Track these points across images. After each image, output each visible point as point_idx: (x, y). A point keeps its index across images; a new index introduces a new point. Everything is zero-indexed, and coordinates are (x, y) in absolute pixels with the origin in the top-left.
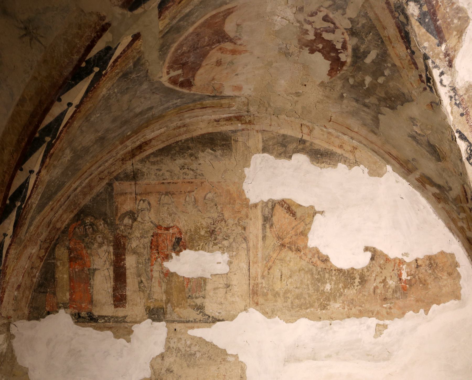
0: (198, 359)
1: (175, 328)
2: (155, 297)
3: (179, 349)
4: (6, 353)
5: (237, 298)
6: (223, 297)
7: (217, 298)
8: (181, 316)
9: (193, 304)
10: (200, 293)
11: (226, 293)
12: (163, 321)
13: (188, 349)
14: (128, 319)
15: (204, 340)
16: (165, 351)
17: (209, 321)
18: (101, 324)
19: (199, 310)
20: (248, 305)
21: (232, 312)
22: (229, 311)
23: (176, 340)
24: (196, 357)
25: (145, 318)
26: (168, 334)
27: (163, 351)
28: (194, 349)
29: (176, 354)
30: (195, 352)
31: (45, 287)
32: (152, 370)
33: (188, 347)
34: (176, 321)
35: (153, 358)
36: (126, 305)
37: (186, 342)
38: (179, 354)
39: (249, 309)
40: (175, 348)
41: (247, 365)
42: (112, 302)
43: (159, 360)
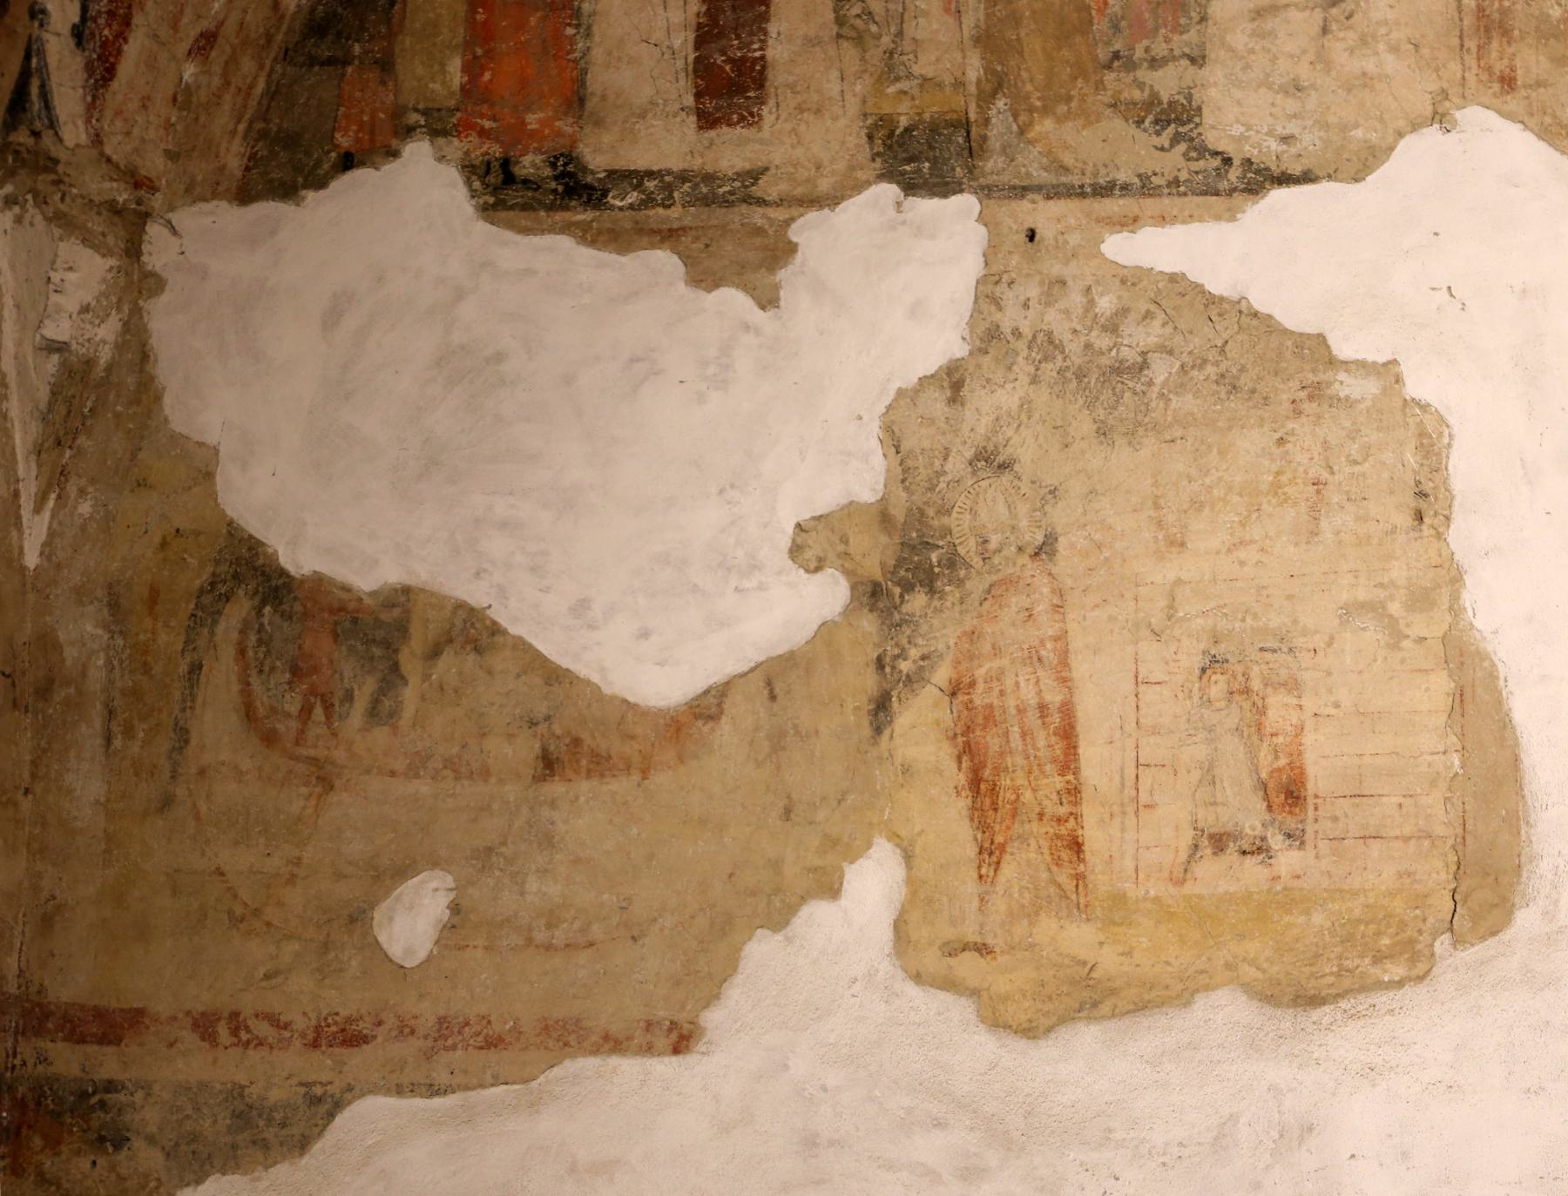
1: (1027, 226)
2: (924, 66)
3: (1051, 342)
4: (109, 369)
5: (1390, 59)
6: (1304, 52)
7: (1274, 59)
8: (1068, 160)
9: (1137, 95)
10: (1176, 38)
11: (1325, 30)
12: (961, 191)
13: (1102, 341)
14: (769, 188)
15: (1199, 288)
16: (971, 353)
17: (1223, 185)
18: (621, 214)
19: (1171, 130)
20: (1454, 91)
21: (1358, 133)
22: (1344, 128)
23: (1033, 291)
24: (1150, 383)
25: (861, 175)
26: (990, 255)
27: (960, 350)
28: (1139, 337)
29: (1032, 369)
30: (1144, 354)
31: (339, 34)
33: (1104, 328)
34: (1038, 188)
35: (900, 393)
36: (765, 110)
37: (1091, 303)
38: (1049, 370)
39: (1458, 115)
40: (1027, 331)
42: (690, 100)
43: (935, 402)
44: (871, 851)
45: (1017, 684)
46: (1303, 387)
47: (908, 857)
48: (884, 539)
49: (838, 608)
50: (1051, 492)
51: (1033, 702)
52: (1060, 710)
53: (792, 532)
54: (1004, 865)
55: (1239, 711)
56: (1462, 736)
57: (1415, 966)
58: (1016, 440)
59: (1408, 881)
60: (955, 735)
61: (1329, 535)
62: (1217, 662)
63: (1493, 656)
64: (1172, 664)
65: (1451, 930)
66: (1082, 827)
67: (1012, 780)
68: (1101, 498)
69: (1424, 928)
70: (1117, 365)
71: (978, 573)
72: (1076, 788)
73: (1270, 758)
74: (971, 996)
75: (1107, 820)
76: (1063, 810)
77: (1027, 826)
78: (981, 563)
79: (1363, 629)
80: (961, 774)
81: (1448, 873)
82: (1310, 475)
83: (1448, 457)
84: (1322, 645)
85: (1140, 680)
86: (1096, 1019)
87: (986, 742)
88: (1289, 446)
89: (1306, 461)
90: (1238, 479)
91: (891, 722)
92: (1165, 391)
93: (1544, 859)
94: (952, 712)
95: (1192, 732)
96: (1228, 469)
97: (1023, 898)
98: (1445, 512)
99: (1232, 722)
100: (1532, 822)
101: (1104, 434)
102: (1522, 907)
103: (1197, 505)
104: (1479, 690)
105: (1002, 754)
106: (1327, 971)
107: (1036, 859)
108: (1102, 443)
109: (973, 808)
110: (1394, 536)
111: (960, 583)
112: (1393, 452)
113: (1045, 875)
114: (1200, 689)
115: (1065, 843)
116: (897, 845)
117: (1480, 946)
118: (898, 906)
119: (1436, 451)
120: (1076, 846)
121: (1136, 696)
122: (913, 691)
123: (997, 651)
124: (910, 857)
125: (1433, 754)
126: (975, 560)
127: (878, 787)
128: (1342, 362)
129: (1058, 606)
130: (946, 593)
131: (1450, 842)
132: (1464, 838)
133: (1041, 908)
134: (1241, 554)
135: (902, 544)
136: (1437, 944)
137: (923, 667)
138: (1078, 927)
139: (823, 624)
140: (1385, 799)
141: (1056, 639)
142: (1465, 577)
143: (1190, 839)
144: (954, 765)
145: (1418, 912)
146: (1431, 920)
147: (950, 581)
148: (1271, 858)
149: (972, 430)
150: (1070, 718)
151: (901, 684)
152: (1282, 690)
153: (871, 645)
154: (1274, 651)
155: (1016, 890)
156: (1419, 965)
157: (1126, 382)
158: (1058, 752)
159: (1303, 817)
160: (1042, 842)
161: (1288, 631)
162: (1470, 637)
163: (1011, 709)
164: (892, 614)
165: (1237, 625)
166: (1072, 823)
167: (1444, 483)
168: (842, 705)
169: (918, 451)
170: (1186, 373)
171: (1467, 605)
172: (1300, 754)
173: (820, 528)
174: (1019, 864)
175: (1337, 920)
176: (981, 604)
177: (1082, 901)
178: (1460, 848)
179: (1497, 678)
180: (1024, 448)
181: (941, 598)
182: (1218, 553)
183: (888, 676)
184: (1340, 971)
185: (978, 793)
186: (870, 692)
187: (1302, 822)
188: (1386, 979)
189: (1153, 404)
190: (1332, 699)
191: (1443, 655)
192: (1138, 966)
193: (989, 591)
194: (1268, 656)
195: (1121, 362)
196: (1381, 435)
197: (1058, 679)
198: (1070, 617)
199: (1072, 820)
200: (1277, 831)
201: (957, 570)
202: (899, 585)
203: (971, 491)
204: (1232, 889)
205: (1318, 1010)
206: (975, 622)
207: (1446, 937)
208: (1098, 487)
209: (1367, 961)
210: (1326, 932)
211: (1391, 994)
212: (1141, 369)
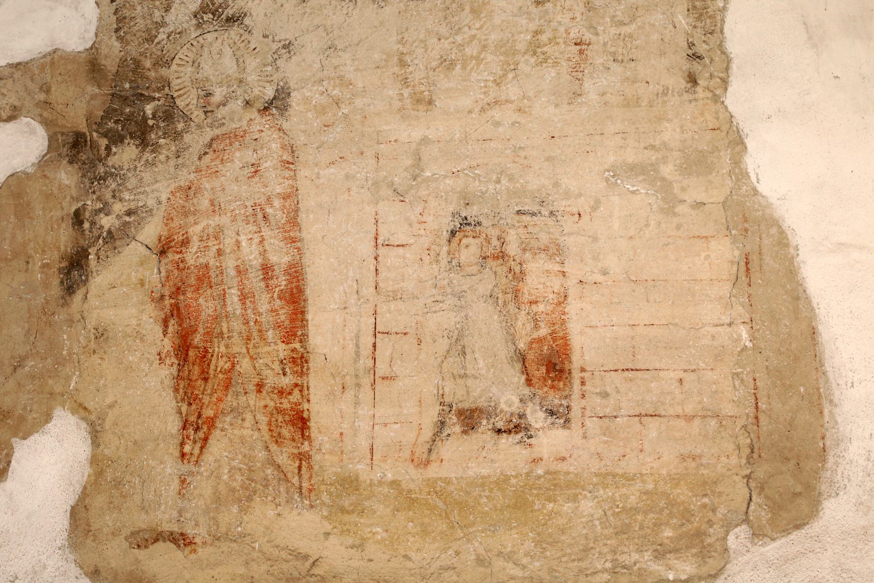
44: (49, 425)
45: (238, 243)
47: (95, 435)
50: (284, 47)
51: (257, 262)
55: (493, 276)
59: (693, 464)
60: (162, 297)
61: (593, 96)
66: (308, 401)
67: (227, 347)
68: (340, 53)
72: (302, 357)
73: (529, 326)
75: (338, 393)
76: (286, 381)
78: (203, 116)
79: (633, 192)
80: (166, 340)
81: (740, 457)
82: (572, 35)
85: (380, 241)
87: (199, 305)
89: (567, 21)
91: (86, 282)
95: (440, 298)
97: (235, 480)
98: (721, 75)
100: (836, 401)
102: (830, 496)
103: (447, 64)
104: (767, 259)
105: (216, 318)
106: (599, 567)
107: (252, 436)
109: (179, 377)
110: (665, 98)
111: (177, 136)
113: (261, 455)
114: (449, 253)
115: (287, 418)
117: (783, 540)
118: (79, 489)
119: (712, 13)
120: (301, 422)
121: (376, 258)
122: (115, 248)
123: (215, 207)
124: (97, 432)
125: (717, 326)
126: (196, 113)
127: (65, 353)
129: (288, 163)
130: (159, 146)
132: (756, 418)
133: (255, 492)
134: (496, 113)
136: (731, 538)
137: (129, 223)
138: (299, 514)
139: (12, 175)
140: (661, 373)
141: (286, 197)
142: (746, 141)
143: (436, 415)
144: (158, 329)
146: (722, 510)
147: (164, 134)
148: (530, 437)
151: (101, 241)
152: (543, 255)
153: (68, 198)
154: (533, 214)
155: (226, 471)
158: (283, 317)
159: (566, 393)
160: (258, 417)
163: (229, 270)
166: (296, 395)
168: (27, 262)
172: (563, 322)
173: (16, 76)
174: (231, 440)
176: (200, 158)
177: (305, 485)
181: (153, 151)
182: (470, 112)
183: (87, 232)
184: (615, 567)
185: (185, 360)
186: (63, 248)
187: (566, 397)
191: (724, 221)
192: (371, 560)
193: (210, 145)
194: (526, 219)
197: (286, 239)
198: (303, 172)
199: (296, 392)
200: (538, 408)
201: (173, 123)
202: (106, 136)
203: (195, 43)
204: (484, 472)
206: (192, 176)
207: (742, 531)
209: (647, 555)
210: (597, 523)
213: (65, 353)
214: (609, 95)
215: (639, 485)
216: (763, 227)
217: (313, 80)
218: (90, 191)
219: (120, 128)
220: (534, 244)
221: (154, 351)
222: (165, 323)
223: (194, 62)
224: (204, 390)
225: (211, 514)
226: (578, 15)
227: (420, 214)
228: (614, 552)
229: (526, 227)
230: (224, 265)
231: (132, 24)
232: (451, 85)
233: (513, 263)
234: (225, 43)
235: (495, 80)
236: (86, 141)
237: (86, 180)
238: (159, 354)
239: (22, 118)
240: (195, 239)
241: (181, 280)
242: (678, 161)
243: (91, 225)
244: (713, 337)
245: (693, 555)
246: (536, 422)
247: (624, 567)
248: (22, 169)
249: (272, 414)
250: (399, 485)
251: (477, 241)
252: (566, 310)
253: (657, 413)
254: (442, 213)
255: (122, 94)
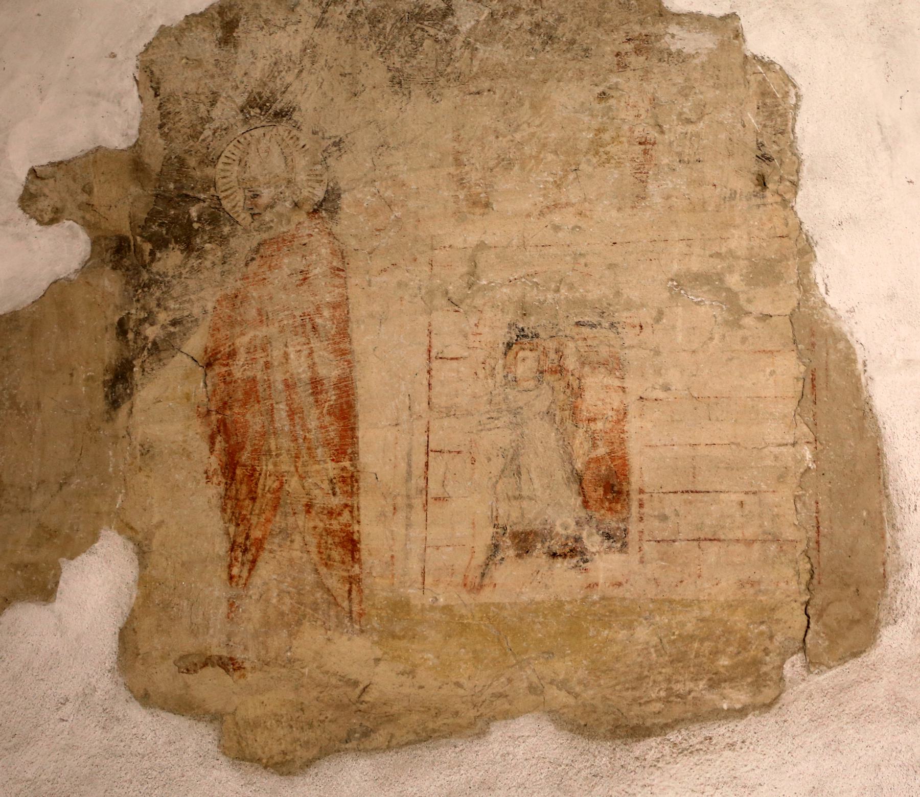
0: (467, 44)
24: (455, 31)
29: (318, 12)
32: (154, 103)
35: (163, 31)
41: (798, 80)
44: (96, 545)
45: (286, 356)
46: (629, 40)
47: (142, 553)
48: (135, 190)
49: (75, 265)
50: (335, 144)
51: (306, 376)
52: (336, 387)
53: (24, 179)
54: (260, 564)
55: (550, 392)
56: (814, 426)
57: (760, 692)
58: (296, 86)
59: (752, 591)
60: (209, 412)
61: (657, 200)
62: (526, 336)
63: (849, 337)
64: (471, 337)
65: (803, 649)
66: (359, 522)
67: (275, 465)
68: (393, 152)
69: (771, 647)
70: (417, 10)
71: (245, 230)
72: (352, 476)
73: (587, 446)
74: (211, 721)
75: (390, 514)
76: (336, 502)
77: (291, 520)
78: (250, 219)
79: (698, 303)
80: (213, 458)
83: (794, 119)
84: (650, 321)
85: (433, 354)
86: (366, 751)
87: (246, 421)
88: (612, 102)
89: (631, 118)
90: (553, 135)
92: (471, 40)
93: (915, 569)
94: (206, 385)
95: (494, 415)
96: (541, 124)
97: (284, 604)
98: (792, 178)
99: (541, 404)
100: (898, 525)
101: (400, 83)
102: (888, 624)
104: (834, 375)
105: (264, 435)
106: (654, 696)
107: (301, 558)
108: (396, 93)
109: (226, 497)
110: (733, 203)
111: (223, 240)
112: (732, 112)
113: (310, 578)
114: (505, 367)
115: (337, 540)
116: (130, 539)
117: (839, 669)
118: (127, 610)
119: (782, 111)
120: (351, 544)
121: (429, 372)
122: (160, 360)
123: (263, 317)
125: (780, 445)
126: (243, 216)
127: (111, 470)
128: (674, 14)
129: (339, 269)
130: (205, 251)
131: (802, 547)
132: (818, 542)
133: (304, 616)
134: (556, 218)
135: (157, 196)
136: (787, 666)
137: (174, 333)
138: (349, 639)
139: (55, 282)
140: (722, 496)
141: (335, 306)
142: (815, 249)
143: (490, 538)
144: (205, 447)
145: (763, 628)
146: (779, 638)
147: (211, 238)
148: (586, 561)
149: (246, 74)
150: (348, 396)
151: (145, 353)
153: (112, 307)
154: (593, 326)
155: (275, 594)
156: (766, 690)
157: (426, 28)
158: (332, 434)
159: (624, 515)
160: (308, 538)
161: (609, 305)
162: (823, 315)
163: (277, 384)
164: (139, 273)
165: (550, 296)
166: (346, 516)
167: (791, 146)
168: (72, 375)
169: (180, 94)
170: (495, 21)
171: (819, 280)
172: (623, 441)
173: (58, 176)
175: (666, 636)
176: (247, 265)
177: (356, 608)
178: (813, 553)
179: (855, 361)
180: (306, 95)
181: (199, 257)
182: (528, 216)
183: (131, 343)
184: (668, 696)
185: (233, 479)
186: (107, 360)
187: (623, 520)
188: (725, 707)
189: (457, 54)
190: (661, 381)
191: (791, 335)
192: (421, 687)
193: (257, 251)
194: (586, 331)
195: (421, 8)
196: (718, 92)
197: (335, 351)
198: (353, 281)
199: (346, 513)
200: (594, 531)
201: (219, 226)
202: (150, 241)
203: (242, 140)
204: (538, 598)
205: (642, 743)
206: (239, 283)
208: (390, 140)
209: (702, 684)
210: (652, 650)
211: (732, 725)
212: (445, 16)
213: (111, 470)
214: (674, 199)
215: (696, 612)
216: (830, 341)
217: (364, 180)
218: (134, 299)
219: (164, 232)
220: (594, 358)
221: (201, 469)
222: (212, 440)
223: (240, 161)
224: (252, 509)
225: (261, 639)
226: (642, 112)
227: (476, 325)
228: (669, 681)
229: (585, 339)
230: (271, 378)
231: (177, 119)
232: (508, 186)
233: (571, 378)
234: (273, 140)
235: (555, 182)
236: (129, 246)
237: (130, 288)
238: (206, 472)
239: (65, 221)
240: (242, 351)
241: (228, 394)
242: (745, 271)
243: (136, 335)
244: (776, 458)
245: (749, 684)
246: (592, 545)
247: (678, 696)
248: (65, 275)
249: (321, 536)
250: (451, 610)
251: (534, 354)
252: (625, 428)
253: (716, 537)
254: (498, 324)
255: (167, 195)
